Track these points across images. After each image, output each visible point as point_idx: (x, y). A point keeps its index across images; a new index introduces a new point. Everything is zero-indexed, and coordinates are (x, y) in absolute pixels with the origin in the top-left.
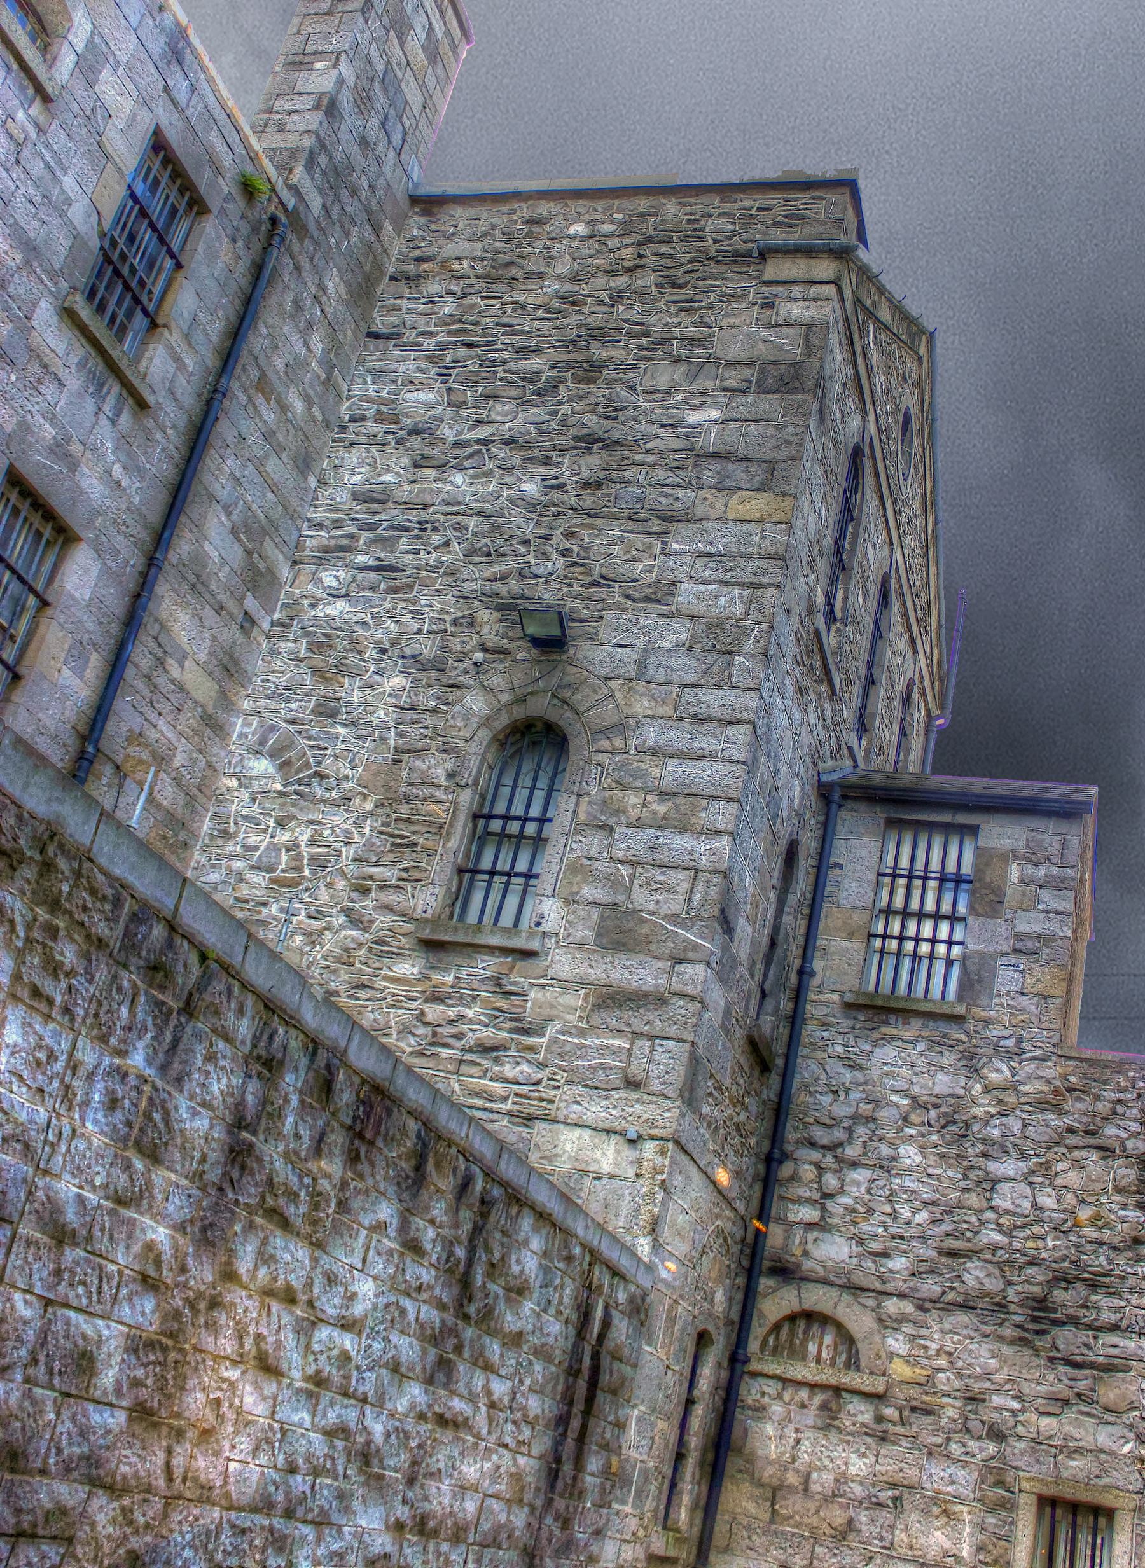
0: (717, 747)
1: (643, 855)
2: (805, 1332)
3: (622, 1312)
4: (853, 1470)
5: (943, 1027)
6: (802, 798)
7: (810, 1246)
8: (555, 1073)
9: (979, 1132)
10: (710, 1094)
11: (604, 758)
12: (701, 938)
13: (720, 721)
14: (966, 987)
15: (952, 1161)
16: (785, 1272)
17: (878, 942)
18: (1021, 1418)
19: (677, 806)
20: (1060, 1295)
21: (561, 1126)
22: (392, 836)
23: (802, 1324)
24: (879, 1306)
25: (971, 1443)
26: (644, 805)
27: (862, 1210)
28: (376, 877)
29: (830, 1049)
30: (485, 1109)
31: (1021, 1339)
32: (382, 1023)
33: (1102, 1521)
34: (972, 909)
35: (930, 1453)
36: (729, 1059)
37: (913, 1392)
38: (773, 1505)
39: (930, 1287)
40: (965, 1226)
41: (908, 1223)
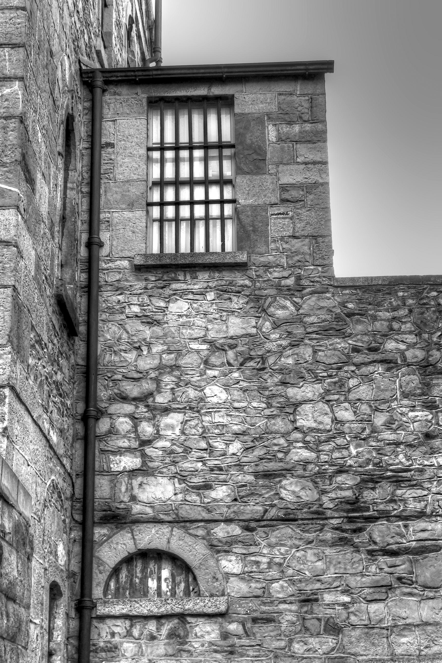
2: (143, 570)
3: (11, 545)
5: (228, 276)
6: (71, 76)
7: (136, 491)
9: (275, 363)
14: (242, 239)
15: (255, 393)
16: (118, 519)
17: (156, 212)
20: (369, 495)
23: (139, 566)
24: (208, 533)
25: (311, 640)
27: (180, 450)
31: (341, 539)
34: (238, 170)
35: (276, 657)
36: (44, 315)
37: (253, 604)
39: (253, 508)
40: (276, 448)
41: (224, 455)
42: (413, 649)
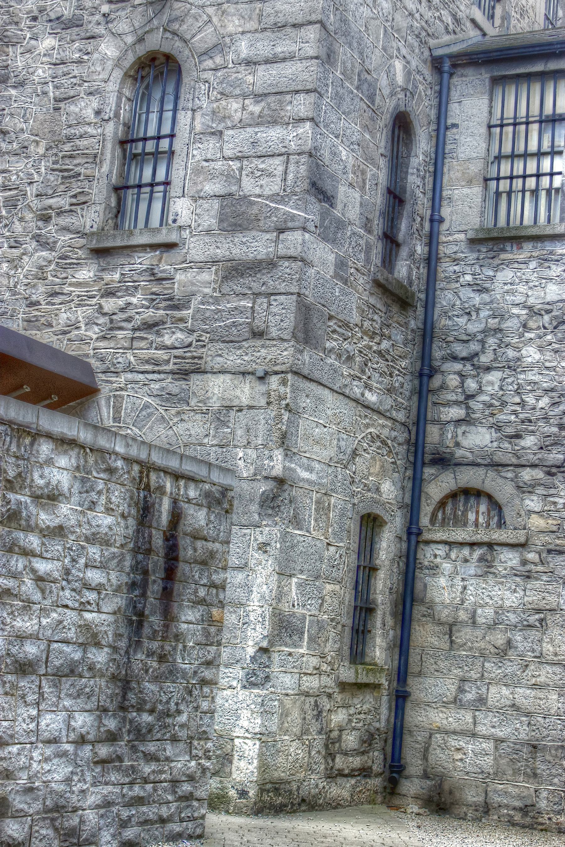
0: (294, 48)
1: (247, 150)
4: (508, 603)
7: (460, 438)
8: (201, 336)
10: (334, 331)
11: (208, 75)
12: (297, 209)
13: (294, 26)
16: (443, 461)
19: (269, 104)
21: (209, 375)
22: (61, 171)
24: (516, 477)
26: (244, 109)
27: (497, 403)
28: (54, 207)
29: (462, 280)
30: (154, 372)
32: (73, 319)
38: (451, 637)
41: (534, 409)
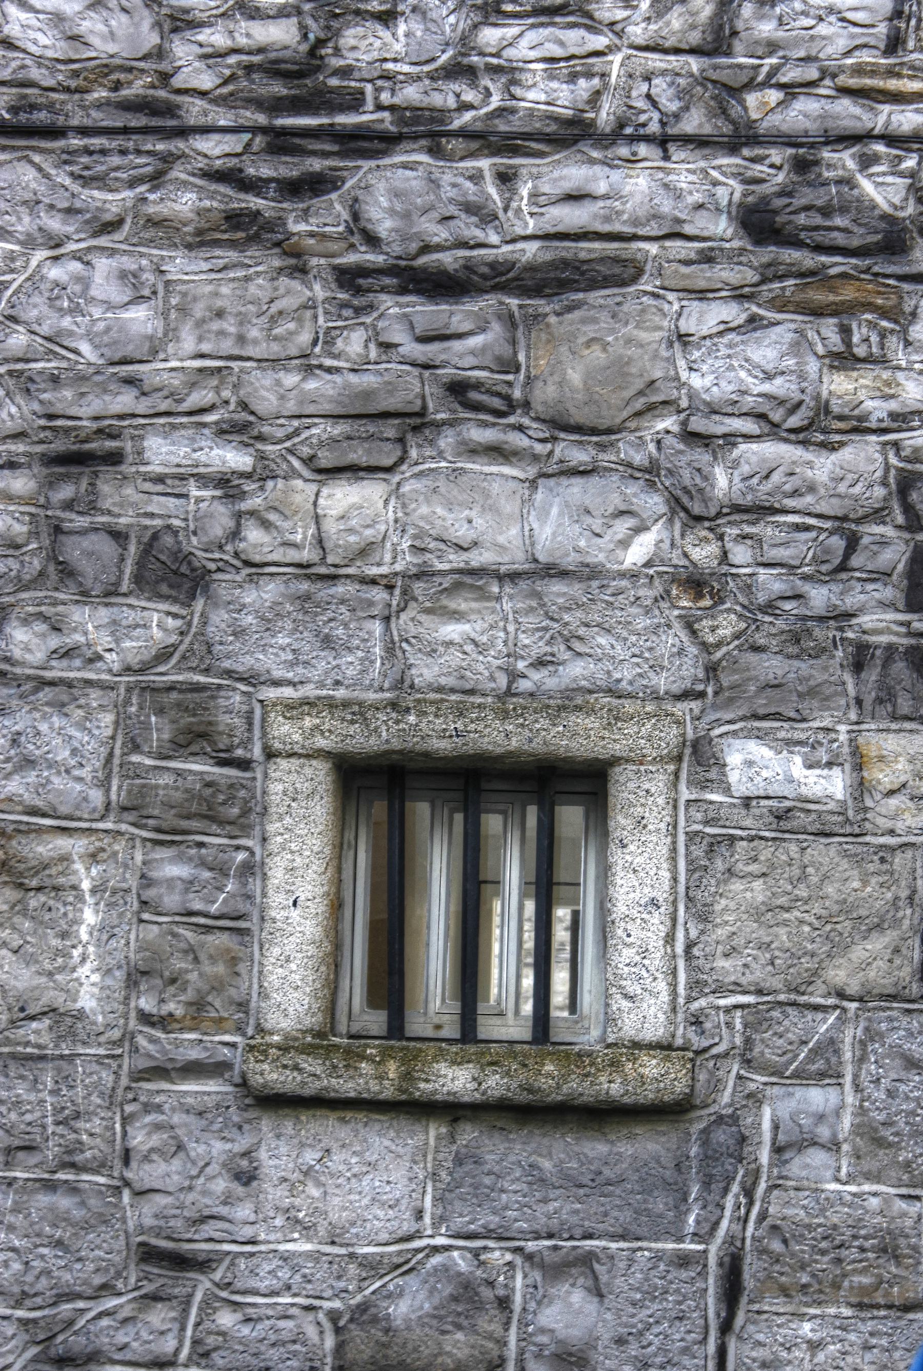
18: (254, 502)
25: (79, 615)
31: (234, 219)
33: (570, 817)
42: (485, 670)
